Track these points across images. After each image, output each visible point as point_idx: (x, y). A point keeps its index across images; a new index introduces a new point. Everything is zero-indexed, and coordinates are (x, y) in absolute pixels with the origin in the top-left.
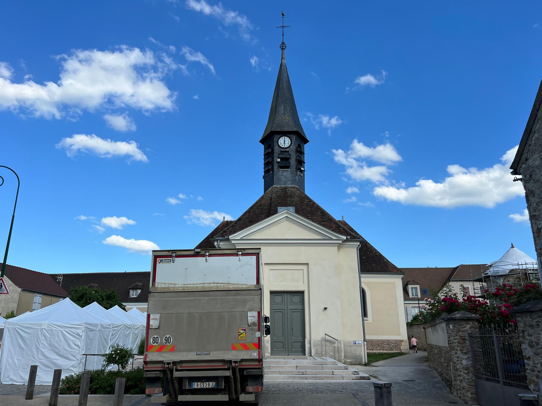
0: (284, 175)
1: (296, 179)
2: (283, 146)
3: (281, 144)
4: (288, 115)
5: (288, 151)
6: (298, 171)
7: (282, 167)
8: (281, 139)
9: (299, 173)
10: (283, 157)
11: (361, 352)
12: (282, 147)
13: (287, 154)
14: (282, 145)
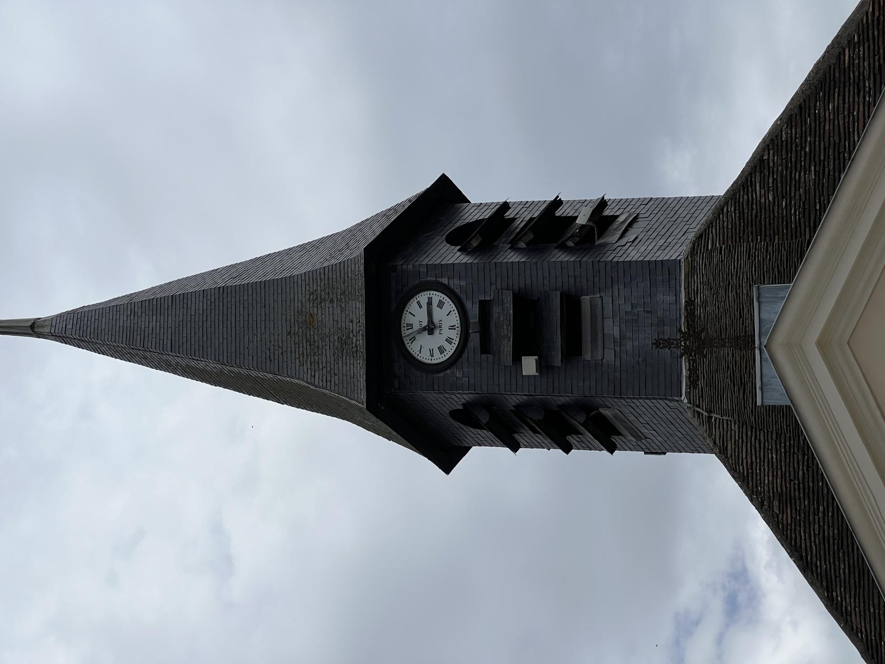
0: (617, 334)
5: (485, 306)
6: (601, 241)
10: (511, 335)
12: (456, 341)
13: (496, 310)
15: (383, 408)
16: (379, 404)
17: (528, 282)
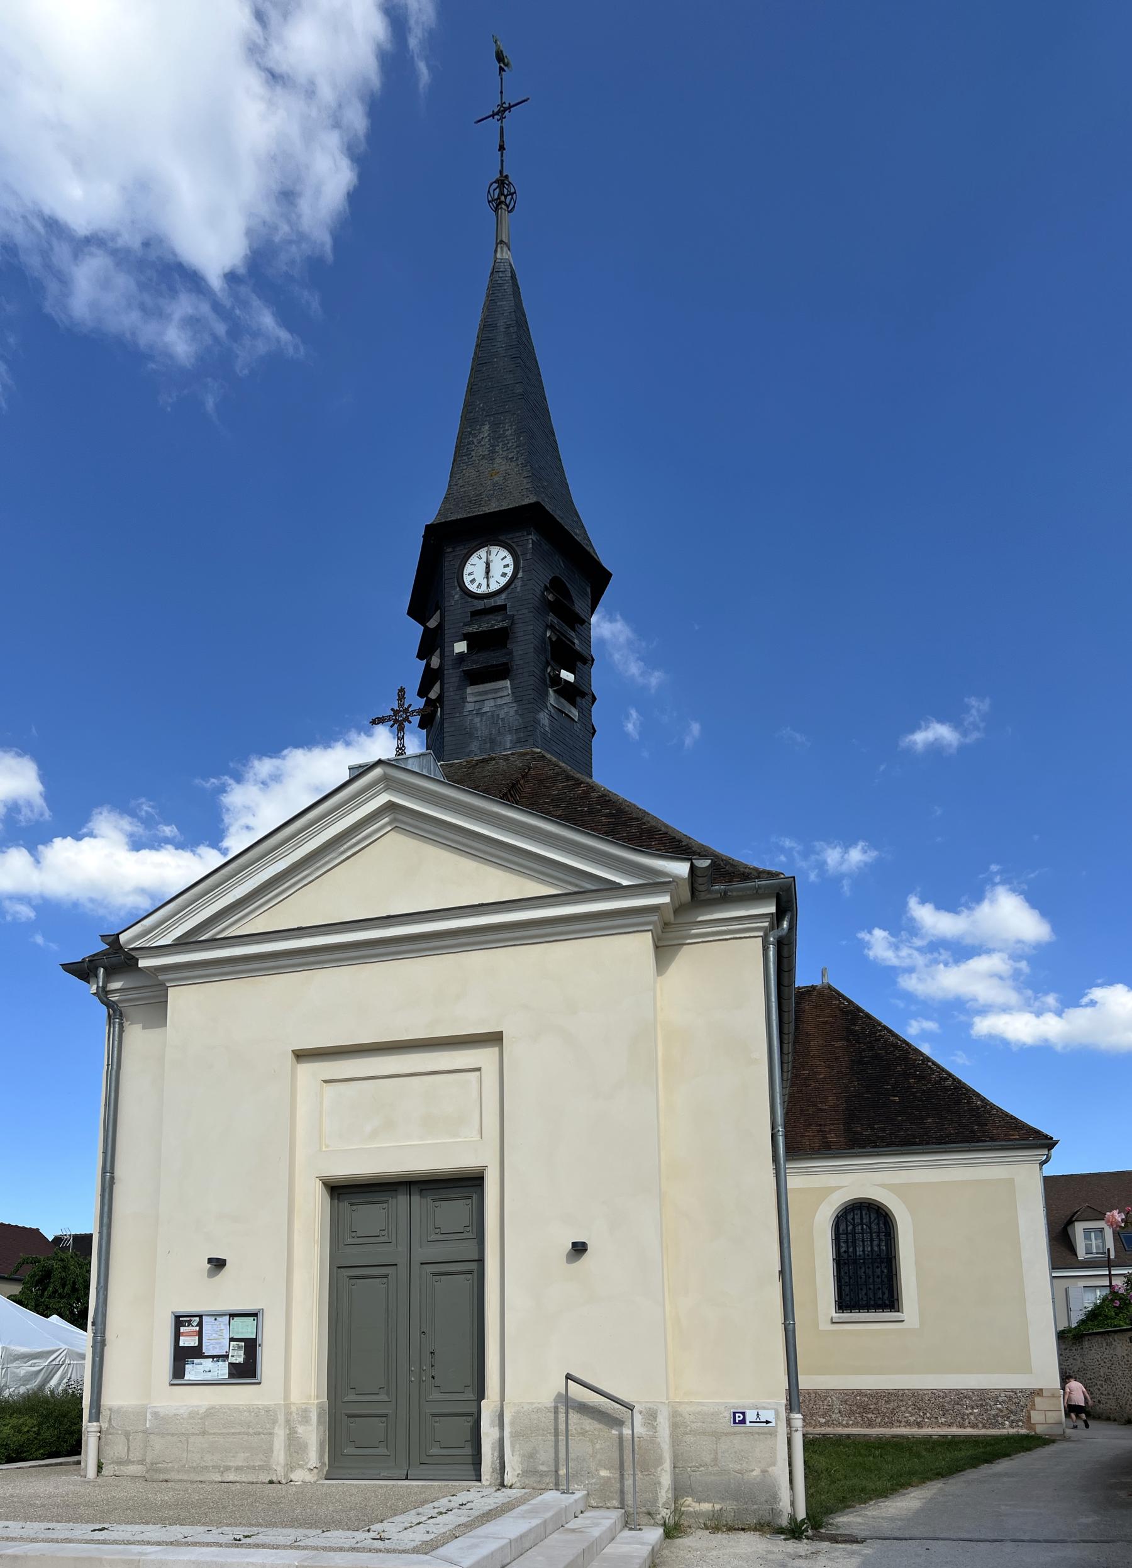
1: (537, 722)
2: (483, 590)
3: (473, 581)
4: (506, 458)
5: (503, 608)
7: (476, 677)
8: (474, 559)
9: (552, 697)
11: (774, 1464)
12: (480, 591)
14: (479, 586)
15: (432, 542)
16: (433, 538)
17: (519, 639)
